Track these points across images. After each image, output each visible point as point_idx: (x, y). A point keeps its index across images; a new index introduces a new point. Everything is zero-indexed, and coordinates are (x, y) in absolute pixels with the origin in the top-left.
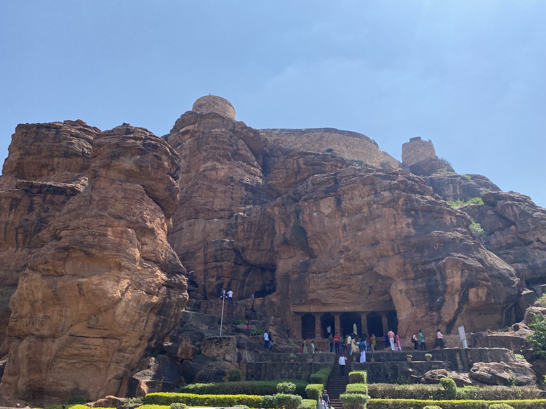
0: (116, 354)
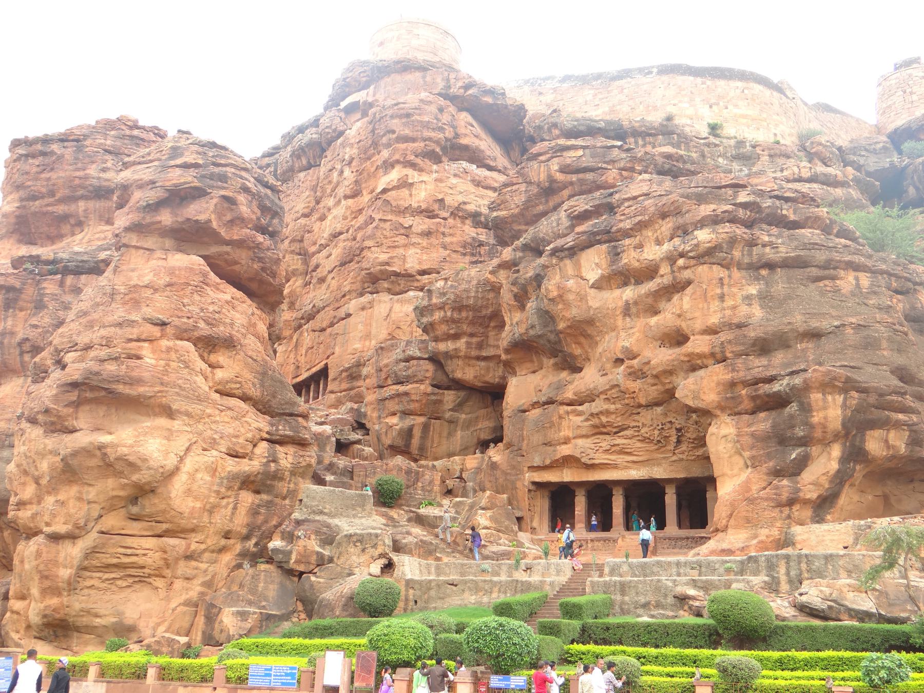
0: (182, 563)
